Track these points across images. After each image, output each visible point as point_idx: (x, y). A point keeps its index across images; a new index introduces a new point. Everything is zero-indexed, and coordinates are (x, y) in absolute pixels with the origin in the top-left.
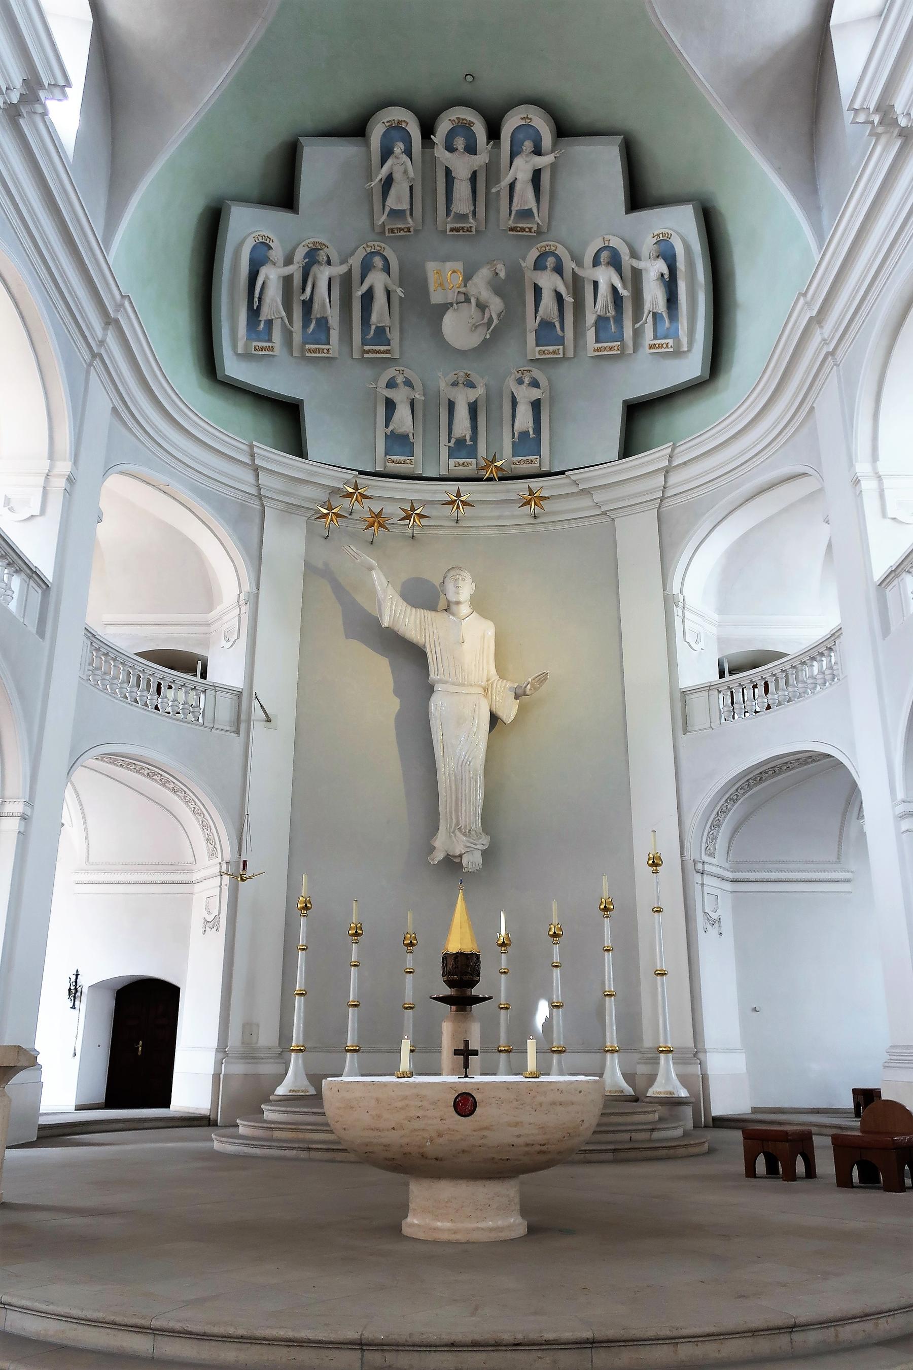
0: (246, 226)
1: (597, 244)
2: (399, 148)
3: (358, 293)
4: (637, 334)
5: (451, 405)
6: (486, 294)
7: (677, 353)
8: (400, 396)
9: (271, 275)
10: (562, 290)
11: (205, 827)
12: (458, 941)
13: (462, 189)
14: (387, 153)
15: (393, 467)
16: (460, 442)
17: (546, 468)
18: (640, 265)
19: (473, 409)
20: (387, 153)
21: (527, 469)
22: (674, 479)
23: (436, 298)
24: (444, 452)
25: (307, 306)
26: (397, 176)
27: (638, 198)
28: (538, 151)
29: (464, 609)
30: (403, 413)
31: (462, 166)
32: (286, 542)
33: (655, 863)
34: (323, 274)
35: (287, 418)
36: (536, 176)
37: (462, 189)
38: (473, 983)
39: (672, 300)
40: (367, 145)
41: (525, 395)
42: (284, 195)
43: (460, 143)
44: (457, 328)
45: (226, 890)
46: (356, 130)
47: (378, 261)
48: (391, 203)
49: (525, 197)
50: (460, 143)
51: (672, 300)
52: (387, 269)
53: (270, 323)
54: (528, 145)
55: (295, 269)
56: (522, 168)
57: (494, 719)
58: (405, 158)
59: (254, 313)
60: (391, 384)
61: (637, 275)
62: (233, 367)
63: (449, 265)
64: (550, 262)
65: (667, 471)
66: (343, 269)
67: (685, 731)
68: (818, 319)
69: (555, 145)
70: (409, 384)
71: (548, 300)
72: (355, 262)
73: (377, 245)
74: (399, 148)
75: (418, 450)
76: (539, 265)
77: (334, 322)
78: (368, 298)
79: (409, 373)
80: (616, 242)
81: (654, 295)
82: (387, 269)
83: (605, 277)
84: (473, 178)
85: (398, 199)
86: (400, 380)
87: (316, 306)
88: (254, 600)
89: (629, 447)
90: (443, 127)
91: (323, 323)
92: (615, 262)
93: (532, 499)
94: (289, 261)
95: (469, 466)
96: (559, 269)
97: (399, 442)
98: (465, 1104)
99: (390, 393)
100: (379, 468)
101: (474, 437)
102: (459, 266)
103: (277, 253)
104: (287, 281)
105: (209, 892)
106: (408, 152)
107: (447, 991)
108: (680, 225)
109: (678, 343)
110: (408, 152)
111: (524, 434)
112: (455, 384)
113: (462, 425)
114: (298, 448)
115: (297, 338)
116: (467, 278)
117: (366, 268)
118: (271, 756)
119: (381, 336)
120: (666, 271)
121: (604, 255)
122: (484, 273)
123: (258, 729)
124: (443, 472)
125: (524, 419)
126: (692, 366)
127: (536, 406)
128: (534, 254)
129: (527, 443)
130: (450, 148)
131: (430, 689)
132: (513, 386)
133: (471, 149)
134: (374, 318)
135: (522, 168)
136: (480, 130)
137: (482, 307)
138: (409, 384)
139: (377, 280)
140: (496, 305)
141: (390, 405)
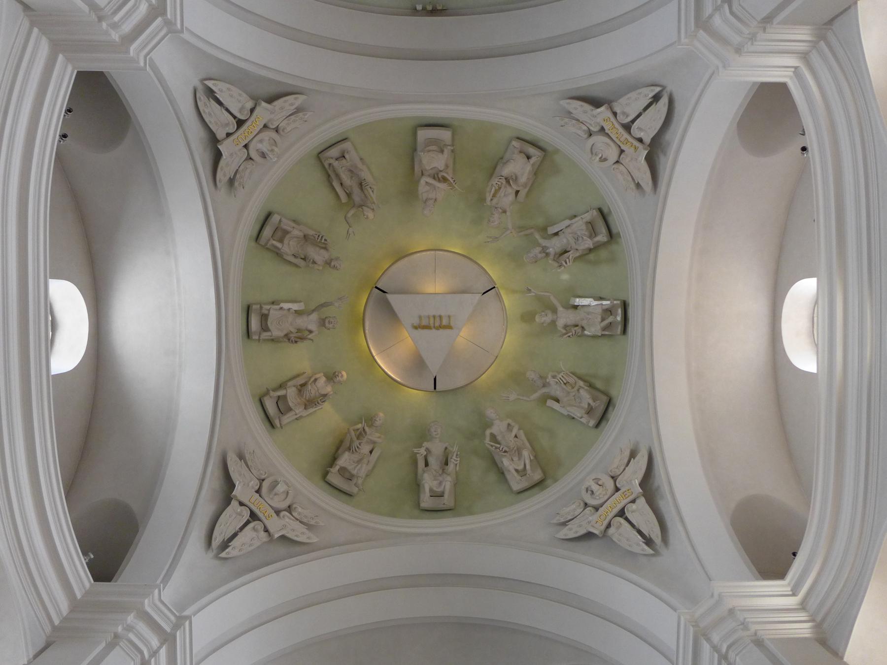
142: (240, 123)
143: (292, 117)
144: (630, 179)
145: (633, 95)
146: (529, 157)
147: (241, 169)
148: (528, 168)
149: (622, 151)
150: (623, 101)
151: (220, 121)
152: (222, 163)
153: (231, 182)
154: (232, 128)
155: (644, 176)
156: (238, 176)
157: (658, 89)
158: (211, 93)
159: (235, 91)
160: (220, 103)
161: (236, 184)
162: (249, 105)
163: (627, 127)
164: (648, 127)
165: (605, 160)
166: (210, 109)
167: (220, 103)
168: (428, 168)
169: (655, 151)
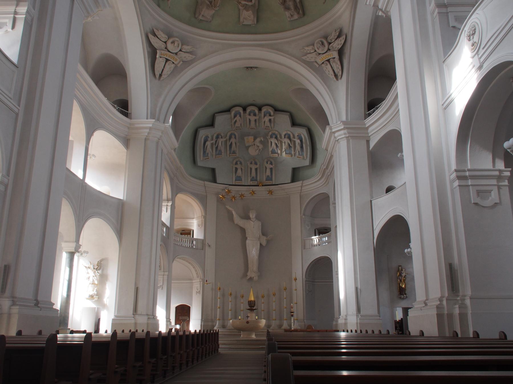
0: (202, 133)
1: (285, 132)
2: (238, 116)
3: (228, 144)
4: (295, 154)
5: (251, 169)
6: (258, 144)
7: (304, 158)
8: (239, 166)
9: (208, 144)
10: (277, 142)
11: (196, 271)
12: (252, 298)
13: (253, 123)
14: (235, 116)
15: (237, 184)
16: (253, 177)
17: (274, 183)
18: (295, 140)
19: (256, 169)
20: (235, 116)
21: (269, 183)
22: (303, 189)
23: (247, 145)
24: (249, 180)
25: (217, 148)
26: (238, 121)
27: (294, 124)
28: (270, 115)
29: (254, 220)
30: (239, 171)
31: (253, 118)
32: (212, 202)
33: (296, 279)
34: (220, 141)
35: (213, 175)
36: (270, 120)
37: (253, 123)
38: (254, 307)
39: (302, 147)
40: (231, 114)
41: (269, 166)
42: (211, 124)
43: (252, 114)
44: (252, 152)
45: (201, 285)
46: (228, 110)
47: (233, 136)
48: (237, 125)
49: (268, 124)
50: (252, 114)
51: (302, 147)
52: (235, 138)
53: (208, 153)
54: (268, 115)
55: (214, 141)
56: (267, 119)
57: (261, 244)
58: (239, 118)
59: (204, 152)
60: (236, 163)
61: (295, 142)
62: (200, 163)
63: (250, 137)
64: (274, 136)
65: (302, 187)
66: (225, 139)
67: (304, 248)
68: (327, 168)
69: (274, 113)
70: (241, 163)
71: (273, 144)
72: (228, 137)
73: (233, 132)
74: (238, 116)
75: (243, 179)
76: (271, 137)
77: (223, 151)
78: (231, 145)
79: (240, 160)
80: (289, 133)
81: (298, 147)
82: (235, 138)
83: (287, 141)
84: (255, 120)
85: (238, 124)
86: (238, 163)
87: (219, 148)
88: (205, 217)
89: (293, 180)
90: (248, 111)
91: (220, 151)
92: (289, 138)
93: (271, 192)
94: (212, 139)
95: (256, 183)
96: (276, 138)
97: (239, 178)
98: (248, 322)
99: (237, 166)
100: (234, 184)
101: (256, 177)
102: (253, 137)
103: (209, 139)
104: (212, 144)
105: (197, 285)
106: (240, 116)
107: (249, 308)
108: (303, 132)
109: (304, 157)
110: (240, 116)
111: (268, 176)
112: (251, 163)
113: (253, 174)
114: (214, 181)
115: (214, 153)
116: (255, 139)
117: (230, 138)
118: (210, 254)
119: (234, 152)
120: (299, 142)
121: (286, 136)
122: (258, 140)
123: (207, 248)
124: (249, 184)
125: (268, 173)
126: (307, 162)
127: (271, 169)
128: (270, 133)
129: (269, 178)
130: (250, 115)
131: (246, 238)
132: (265, 163)
133: (255, 115)
134: (232, 149)
135: (267, 119)
136: (257, 111)
137: (258, 147)
138: (241, 163)
139: (233, 140)
140: (261, 147)
141: (236, 169)
142: (328, 61)
143: (308, 52)
144: (159, 37)
145: (169, 73)
146: (203, 16)
147: (333, 40)
148: (202, 13)
149: (166, 48)
150: (172, 69)
151: (337, 66)
152: (340, 47)
153: (339, 36)
154: (331, 61)
155: (154, 41)
156: (336, 37)
157: (162, 79)
158: (336, 76)
159: (327, 72)
160: (333, 70)
161: (337, 34)
162: (323, 65)
163: (167, 60)
164: (160, 63)
165: (172, 43)
166: (338, 71)
167: (333, 70)
168: (250, 12)
169: (153, 54)
